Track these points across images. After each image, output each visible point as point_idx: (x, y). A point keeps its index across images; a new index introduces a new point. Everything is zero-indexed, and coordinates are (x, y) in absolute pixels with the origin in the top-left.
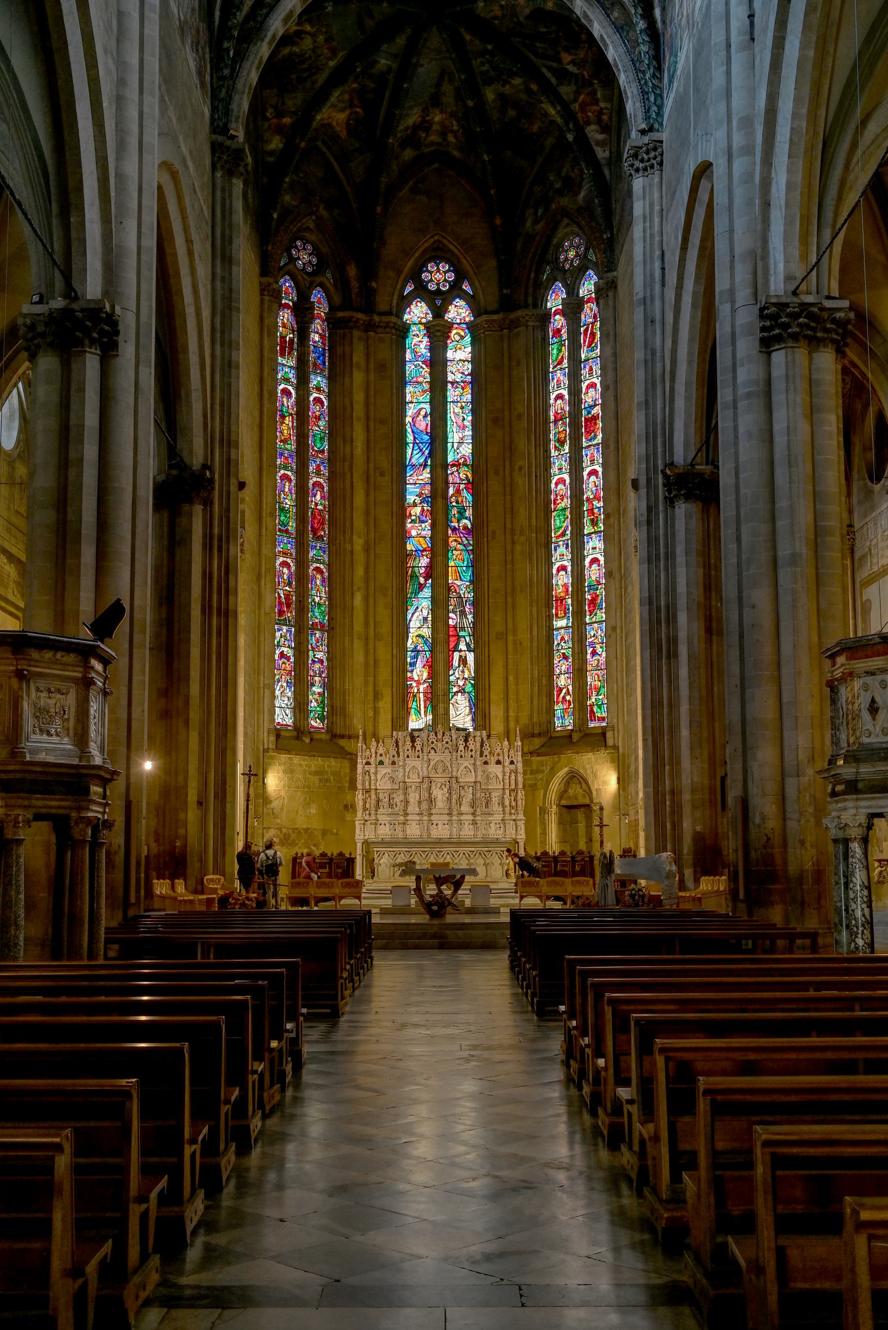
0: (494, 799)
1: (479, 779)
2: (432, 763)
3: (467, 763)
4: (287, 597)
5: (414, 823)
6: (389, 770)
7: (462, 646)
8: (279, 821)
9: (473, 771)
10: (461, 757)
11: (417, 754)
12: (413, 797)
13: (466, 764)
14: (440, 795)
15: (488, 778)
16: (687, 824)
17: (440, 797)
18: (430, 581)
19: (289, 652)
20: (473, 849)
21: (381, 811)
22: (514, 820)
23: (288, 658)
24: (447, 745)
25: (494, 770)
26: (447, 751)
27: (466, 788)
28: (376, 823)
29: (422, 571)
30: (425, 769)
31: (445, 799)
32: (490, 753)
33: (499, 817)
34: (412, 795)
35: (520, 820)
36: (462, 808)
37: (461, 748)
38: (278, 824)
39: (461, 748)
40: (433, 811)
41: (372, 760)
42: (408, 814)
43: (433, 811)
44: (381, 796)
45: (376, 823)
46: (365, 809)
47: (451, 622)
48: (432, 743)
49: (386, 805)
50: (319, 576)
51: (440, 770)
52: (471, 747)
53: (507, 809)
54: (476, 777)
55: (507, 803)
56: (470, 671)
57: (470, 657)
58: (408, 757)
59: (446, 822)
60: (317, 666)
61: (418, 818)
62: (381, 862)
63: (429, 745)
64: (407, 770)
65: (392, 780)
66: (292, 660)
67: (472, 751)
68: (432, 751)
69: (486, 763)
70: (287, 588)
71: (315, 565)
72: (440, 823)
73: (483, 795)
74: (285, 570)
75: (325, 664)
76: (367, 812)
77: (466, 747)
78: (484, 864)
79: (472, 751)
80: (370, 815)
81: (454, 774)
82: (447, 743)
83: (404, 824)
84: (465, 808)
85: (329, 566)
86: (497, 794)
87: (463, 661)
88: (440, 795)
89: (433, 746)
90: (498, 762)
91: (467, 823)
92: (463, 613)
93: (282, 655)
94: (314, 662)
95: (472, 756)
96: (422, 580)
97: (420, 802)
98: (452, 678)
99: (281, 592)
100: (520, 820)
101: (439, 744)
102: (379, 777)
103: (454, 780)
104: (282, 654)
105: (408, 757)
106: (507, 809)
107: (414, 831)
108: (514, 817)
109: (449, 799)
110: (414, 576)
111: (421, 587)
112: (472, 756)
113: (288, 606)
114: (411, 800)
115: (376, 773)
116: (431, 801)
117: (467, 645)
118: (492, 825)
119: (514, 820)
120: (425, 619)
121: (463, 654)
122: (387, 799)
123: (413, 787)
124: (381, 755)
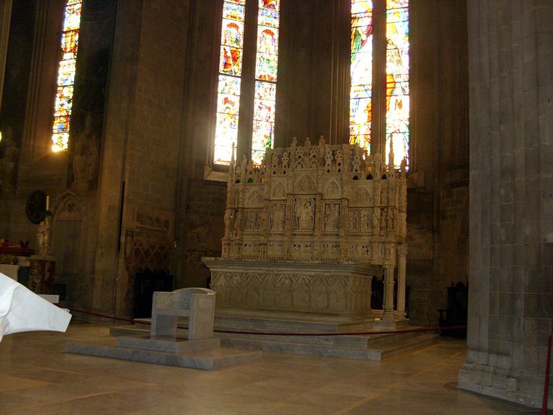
0: (363, 219)
2: (299, 179)
4: (233, 52)
6: (256, 188)
7: (398, 91)
9: (340, 188)
10: (329, 171)
11: (283, 169)
14: (304, 213)
17: (303, 216)
18: (371, 37)
19: (236, 100)
20: (313, 273)
21: (249, 231)
22: (383, 243)
23: (233, 104)
24: (314, 160)
25: (364, 186)
26: (314, 165)
27: (332, 205)
29: (365, 29)
31: (309, 218)
32: (361, 168)
34: (276, 213)
35: (390, 242)
37: (329, 161)
39: (329, 161)
40: (297, 232)
41: (241, 179)
42: (270, 235)
43: (297, 232)
46: (232, 228)
47: (388, 71)
48: (300, 157)
50: (269, 37)
52: (339, 160)
54: (342, 193)
55: (376, 222)
56: (405, 112)
57: (406, 101)
58: (274, 173)
59: (308, 244)
60: (264, 113)
61: (280, 239)
63: (296, 160)
65: (260, 198)
66: (237, 105)
67: (340, 164)
69: (356, 178)
70: (235, 45)
71: (265, 28)
72: (302, 245)
74: (233, 30)
75: (273, 110)
76: (234, 232)
77: (334, 161)
79: (340, 164)
81: (320, 190)
82: (314, 156)
83: (266, 244)
84: (330, 229)
85: (281, 29)
87: (400, 105)
88: (304, 213)
90: (369, 177)
92: (399, 62)
93: (226, 100)
94: (261, 108)
95: (339, 171)
96: (364, 37)
98: (388, 121)
99: (228, 49)
100: (390, 242)
101: (306, 159)
102: (247, 195)
103: (318, 197)
104: (226, 100)
105: (274, 173)
107: (274, 251)
110: (357, 34)
111: (363, 42)
112: (339, 171)
113: (235, 59)
115: (243, 191)
117: (403, 90)
118: (360, 248)
119: (383, 243)
120: (366, 69)
121: (399, 99)
123: (278, 205)
124: (251, 173)
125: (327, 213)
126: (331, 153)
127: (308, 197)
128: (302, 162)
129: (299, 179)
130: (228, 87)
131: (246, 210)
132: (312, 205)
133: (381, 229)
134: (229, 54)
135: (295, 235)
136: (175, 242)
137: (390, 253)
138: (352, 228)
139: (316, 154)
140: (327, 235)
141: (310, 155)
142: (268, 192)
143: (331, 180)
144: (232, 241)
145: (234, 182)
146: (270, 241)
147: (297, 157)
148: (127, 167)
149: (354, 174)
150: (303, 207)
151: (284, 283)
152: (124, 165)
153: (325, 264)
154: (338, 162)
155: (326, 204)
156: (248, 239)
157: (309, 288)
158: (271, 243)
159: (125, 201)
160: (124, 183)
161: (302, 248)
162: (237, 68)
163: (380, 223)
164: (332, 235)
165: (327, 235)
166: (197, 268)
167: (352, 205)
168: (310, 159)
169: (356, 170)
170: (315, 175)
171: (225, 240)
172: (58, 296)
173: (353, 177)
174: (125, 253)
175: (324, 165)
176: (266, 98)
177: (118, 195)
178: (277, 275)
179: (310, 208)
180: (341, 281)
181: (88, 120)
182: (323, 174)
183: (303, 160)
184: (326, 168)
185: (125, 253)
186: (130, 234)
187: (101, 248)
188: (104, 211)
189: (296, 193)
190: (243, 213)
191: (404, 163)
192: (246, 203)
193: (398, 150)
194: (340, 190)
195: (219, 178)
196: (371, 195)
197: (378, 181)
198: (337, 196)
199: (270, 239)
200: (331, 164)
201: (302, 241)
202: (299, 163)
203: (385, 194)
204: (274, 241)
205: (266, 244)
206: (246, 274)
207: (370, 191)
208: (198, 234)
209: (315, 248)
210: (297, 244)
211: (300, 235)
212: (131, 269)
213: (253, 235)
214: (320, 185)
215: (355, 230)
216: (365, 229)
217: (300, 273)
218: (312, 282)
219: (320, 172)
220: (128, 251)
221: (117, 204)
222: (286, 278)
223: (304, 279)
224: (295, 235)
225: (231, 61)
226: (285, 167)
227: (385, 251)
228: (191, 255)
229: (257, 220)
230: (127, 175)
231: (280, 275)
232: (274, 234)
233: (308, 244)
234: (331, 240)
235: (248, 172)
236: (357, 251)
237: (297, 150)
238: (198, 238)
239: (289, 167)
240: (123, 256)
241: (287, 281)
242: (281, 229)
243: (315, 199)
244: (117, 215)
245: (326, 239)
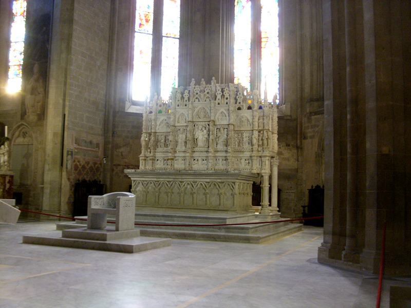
0: (245, 139)
1: (232, 121)
2: (196, 110)
3: (223, 109)
5: (180, 159)
8: (126, 160)
9: (227, 115)
10: (219, 104)
11: (185, 103)
12: (181, 137)
13: (222, 110)
14: (201, 135)
15: (241, 121)
16: (370, 144)
20: (208, 180)
21: (159, 149)
24: (208, 95)
25: (246, 115)
26: (208, 100)
27: (222, 129)
28: (154, 159)
30: (190, 116)
32: (243, 101)
33: (247, 154)
34: (180, 136)
35: (265, 156)
36: (218, 146)
37: (219, 97)
38: (126, 163)
39: (219, 97)
40: (196, 149)
44: (160, 139)
45: (154, 159)
46: (147, 147)
48: (197, 94)
49: (163, 145)
51: (202, 115)
52: (227, 95)
53: (256, 147)
55: (255, 141)
58: (178, 106)
59: (204, 158)
61: (183, 155)
62: (138, 189)
63: (194, 96)
64: (177, 116)
65: (168, 125)
67: (227, 98)
68: (197, 100)
69: (239, 109)
72: (200, 159)
73: (236, 135)
76: (149, 150)
77: (223, 96)
78: (218, 194)
80: (150, 152)
81: (212, 118)
82: (208, 93)
83: (172, 159)
84: (220, 147)
86: (248, 135)
88: (201, 135)
89: (197, 96)
90: (250, 108)
91: (221, 160)
95: (227, 103)
97: (186, 142)
100: (265, 156)
101: (202, 95)
103: (211, 124)
105: (178, 106)
106: (256, 147)
107: (179, 165)
108: (260, 154)
109: (208, 140)
112: (227, 103)
113: (147, 21)
114: (180, 140)
116: (195, 141)
118: (243, 161)
119: (260, 157)
122: (163, 141)
123: (181, 130)
125: (219, 135)
126: (220, 90)
127: (204, 123)
128: (198, 97)
129: (196, 110)
130: (142, 42)
131: (157, 134)
132: (207, 129)
133: (258, 147)
134: (143, 17)
135: (194, 152)
136: (105, 159)
137: (265, 164)
138: (237, 146)
139: (209, 91)
140: (218, 151)
141: (205, 91)
142: (174, 121)
143: (221, 111)
144: (147, 157)
145: (148, 113)
146: (175, 157)
147: (195, 94)
148: (67, 103)
149: (238, 106)
150: (200, 131)
151: (186, 188)
152: (64, 100)
153: (217, 174)
154: (225, 97)
155: (217, 129)
156: (158, 155)
157: (205, 191)
158: (177, 158)
159: (66, 129)
160: (65, 115)
161: (200, 161)
162: (149, 27)
163: (258, 142)
164: (222, 151)
165: (218, 151)
166: (121, 178)
167: (237, 129)
168: (205, 95)
169: (240, 103)
170: (209, 106)
171: (142, 156)
172: (14, 200)
173: (237, 108)
174: (67, 168)
175: (215, 100)
176: (171, 50)
177: (60, 124)
178: (181, 182)
179: (205, 131)
180: (229, 185)
181: (36, 68)
182: (215, 106)
183: (200, 96)
184: (217, 101)
185: (67, 168)
186: (71, 153)
187: (49, 164)
188: (50, 137)
189: (194, 120)
190: (155, 136)
191: (275, 97)
192: (157, 129)
193: (271, 89)
194: (227, 117)
195: (137, 110)
196: (251, 121)
197: (256, 111)
198: (226, 122)
199: (176, 155)
200: (220, 98)
201: (199, 157)
202: (197, 98)
203: (261, 120)
204: (178, 157)
205: (172, 159)
206: (158, 182)
207: (250, 119)
208: (122, 152)
209: (210, 161)
210: (196, 158)
211: (199, 152)
212: (72, 180)
213: (163, 152)
214: (212, 114)
215: (239, 148)
216: (246, 146)
217: (199, 180)
218: (207, 186)
219: (212, 105)
220: (69, 167)
221: (60, 131)
222: (188, 184)
223: (201, 184)
224: (194, 152)
225: (144, 22)
226: (186, 101)
227: (262, 163)
228: (117, 168)
229: (165, 141)
230: (67, 109)
231: (183, 182)
232: (179, 152)
233: (204, 158)
234: (221, 155)
235: (158, 105)
236: (241, 163)
237: (195, 88)
238: (122, 155)
239: (189, 101)
240: (65, 170)
241: (189, 187)
242: (184, 148)
243: (209, 125)
244: (59, 139)
245: (218, 154)
